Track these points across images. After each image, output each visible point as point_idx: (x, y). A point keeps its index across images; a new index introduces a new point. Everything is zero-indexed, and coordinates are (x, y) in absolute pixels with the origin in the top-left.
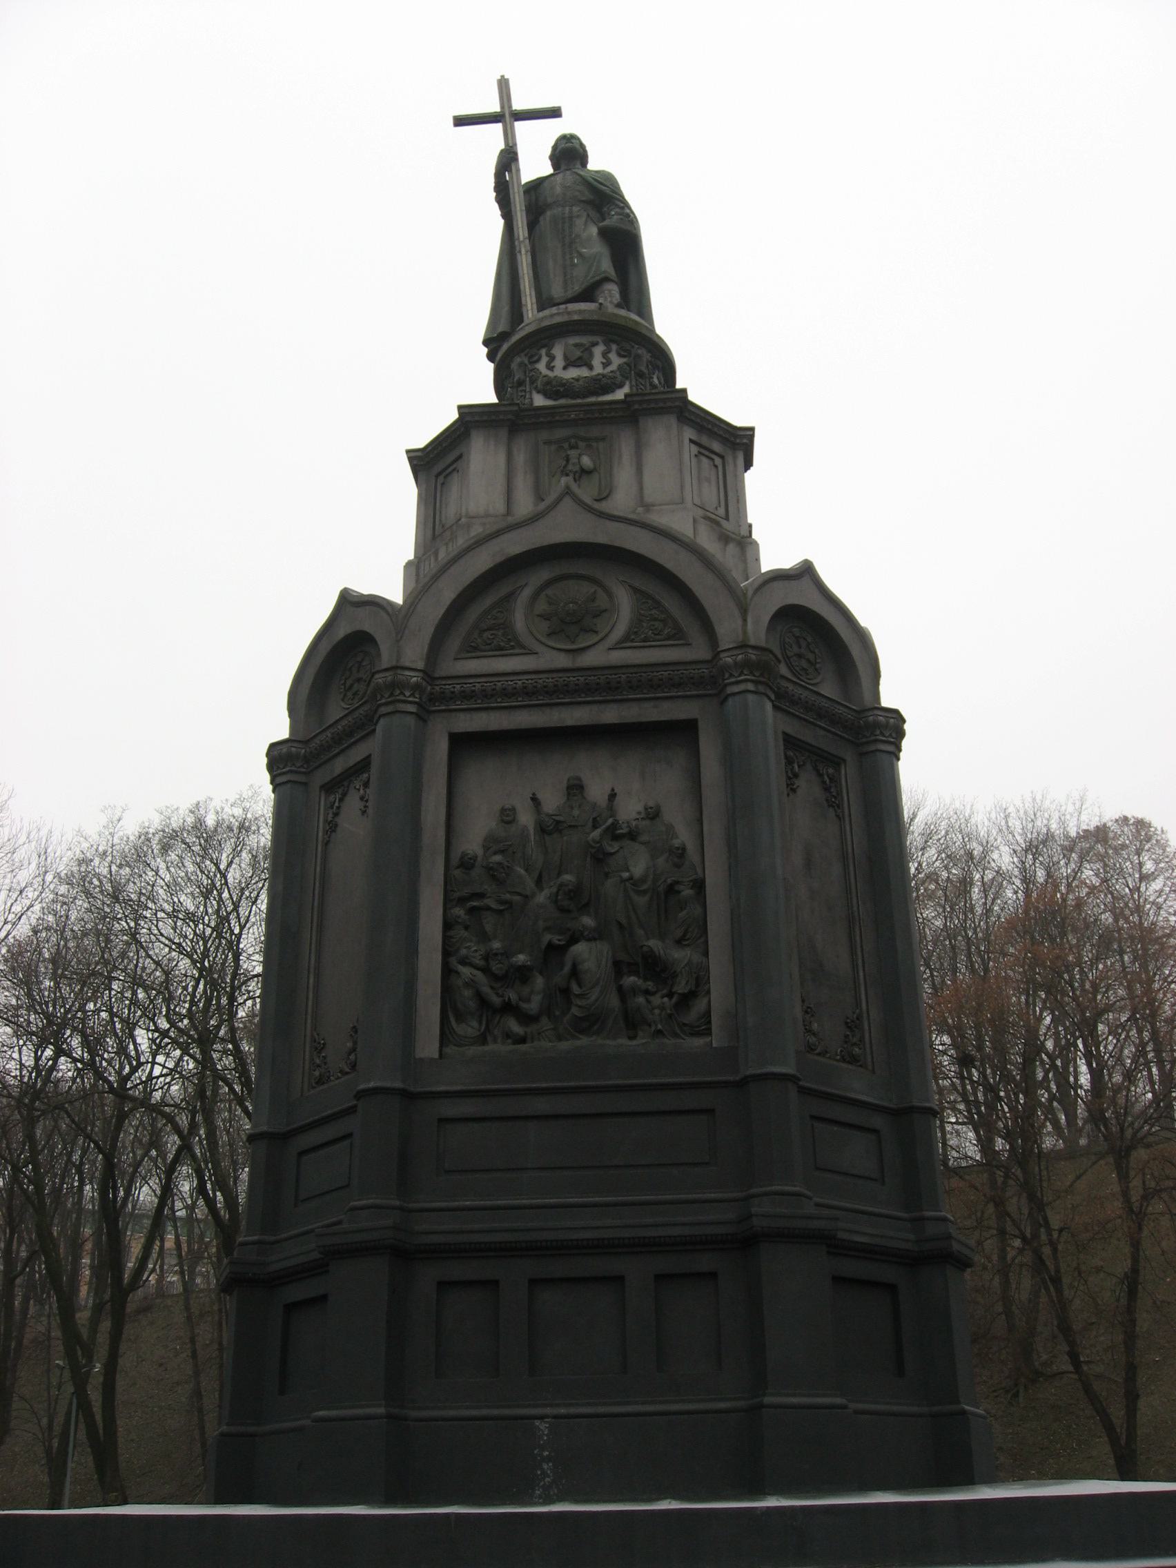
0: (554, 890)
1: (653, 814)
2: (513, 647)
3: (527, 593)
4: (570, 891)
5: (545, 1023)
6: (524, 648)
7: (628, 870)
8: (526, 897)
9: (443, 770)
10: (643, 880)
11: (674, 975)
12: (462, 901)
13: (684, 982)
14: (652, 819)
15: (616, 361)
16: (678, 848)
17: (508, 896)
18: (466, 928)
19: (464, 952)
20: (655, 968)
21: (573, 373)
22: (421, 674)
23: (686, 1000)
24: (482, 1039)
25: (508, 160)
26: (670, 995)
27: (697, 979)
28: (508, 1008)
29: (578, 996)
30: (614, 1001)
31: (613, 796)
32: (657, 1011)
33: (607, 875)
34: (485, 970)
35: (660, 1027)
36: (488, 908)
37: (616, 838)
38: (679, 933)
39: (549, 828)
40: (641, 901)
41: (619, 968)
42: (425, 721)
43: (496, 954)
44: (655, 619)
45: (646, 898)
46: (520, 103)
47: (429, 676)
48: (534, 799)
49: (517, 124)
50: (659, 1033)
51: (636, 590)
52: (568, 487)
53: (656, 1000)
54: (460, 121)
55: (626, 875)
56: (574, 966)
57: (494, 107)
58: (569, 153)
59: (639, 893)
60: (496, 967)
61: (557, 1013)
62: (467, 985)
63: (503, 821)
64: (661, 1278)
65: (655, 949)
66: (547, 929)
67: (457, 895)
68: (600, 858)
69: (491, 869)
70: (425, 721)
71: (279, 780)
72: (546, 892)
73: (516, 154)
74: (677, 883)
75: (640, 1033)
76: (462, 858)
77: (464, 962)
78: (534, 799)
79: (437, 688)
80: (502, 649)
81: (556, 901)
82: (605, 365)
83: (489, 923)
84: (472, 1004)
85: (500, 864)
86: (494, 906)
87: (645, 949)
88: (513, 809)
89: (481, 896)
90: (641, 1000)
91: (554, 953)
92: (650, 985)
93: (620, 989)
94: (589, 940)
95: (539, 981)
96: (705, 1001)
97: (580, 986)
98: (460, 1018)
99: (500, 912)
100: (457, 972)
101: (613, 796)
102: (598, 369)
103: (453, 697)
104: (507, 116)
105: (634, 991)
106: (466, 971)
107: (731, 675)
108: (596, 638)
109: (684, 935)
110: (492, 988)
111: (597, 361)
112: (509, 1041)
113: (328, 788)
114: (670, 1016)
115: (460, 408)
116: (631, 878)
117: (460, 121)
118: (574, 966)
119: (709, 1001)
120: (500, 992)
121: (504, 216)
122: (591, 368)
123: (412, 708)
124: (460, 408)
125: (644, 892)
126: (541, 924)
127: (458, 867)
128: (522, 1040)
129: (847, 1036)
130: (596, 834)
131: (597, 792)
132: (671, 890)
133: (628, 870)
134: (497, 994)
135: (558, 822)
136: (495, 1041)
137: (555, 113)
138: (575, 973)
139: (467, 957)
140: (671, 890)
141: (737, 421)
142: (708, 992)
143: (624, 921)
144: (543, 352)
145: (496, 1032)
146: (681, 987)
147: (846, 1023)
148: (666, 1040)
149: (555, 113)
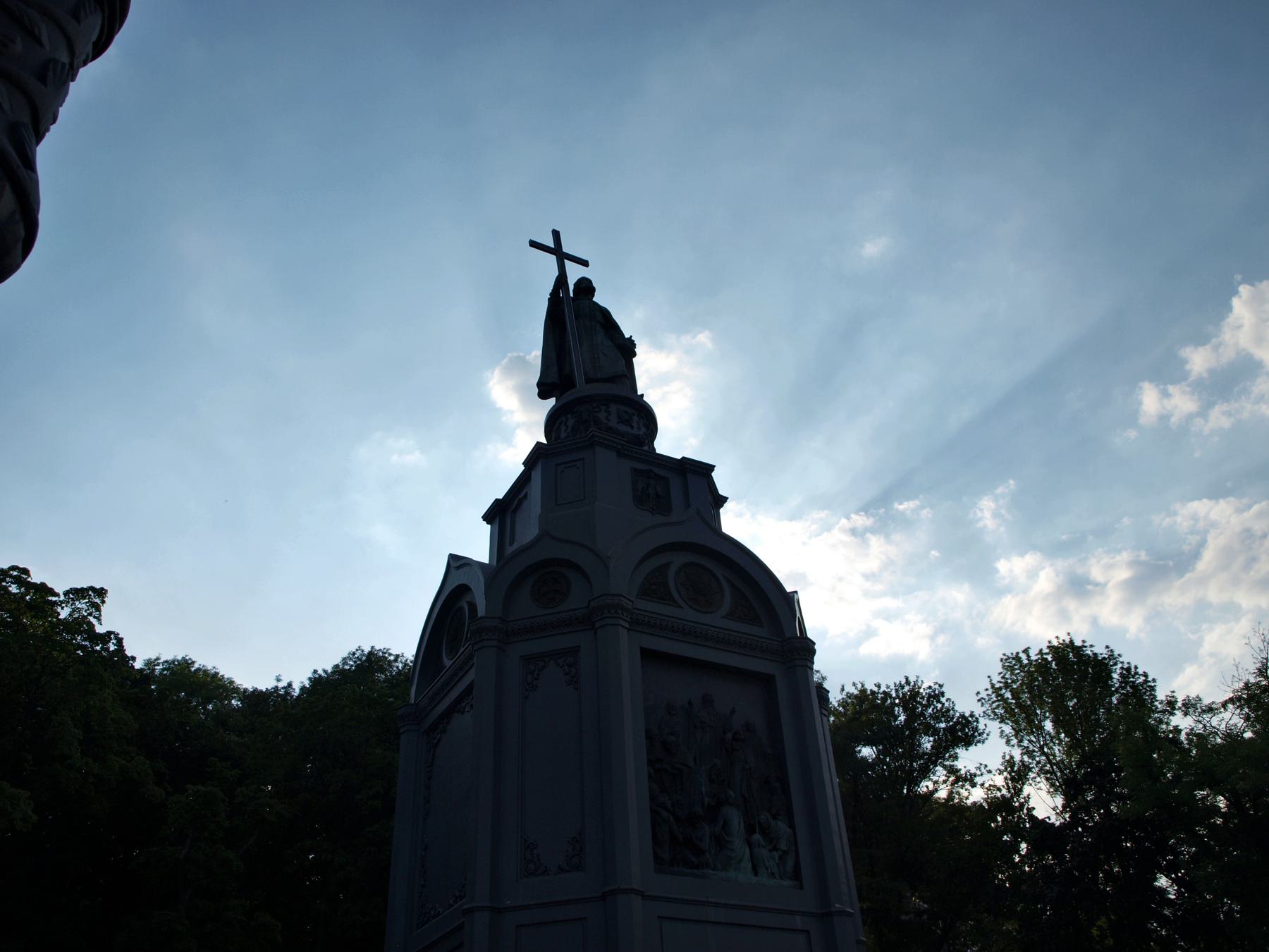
15: (643, 430)
21: (623, 428)
25: (561, 280)
46: (566, 249)
54: (534, 244)
57: (550, 243)
58: (585, 287)
82: (639, 429)
102: (635, 432)
111: (635, 425)
117: (534, 244)
122: (632, 427)
137: (585, 263)
141: (722, 491)
144: (604, 408)
149: (585, 263)
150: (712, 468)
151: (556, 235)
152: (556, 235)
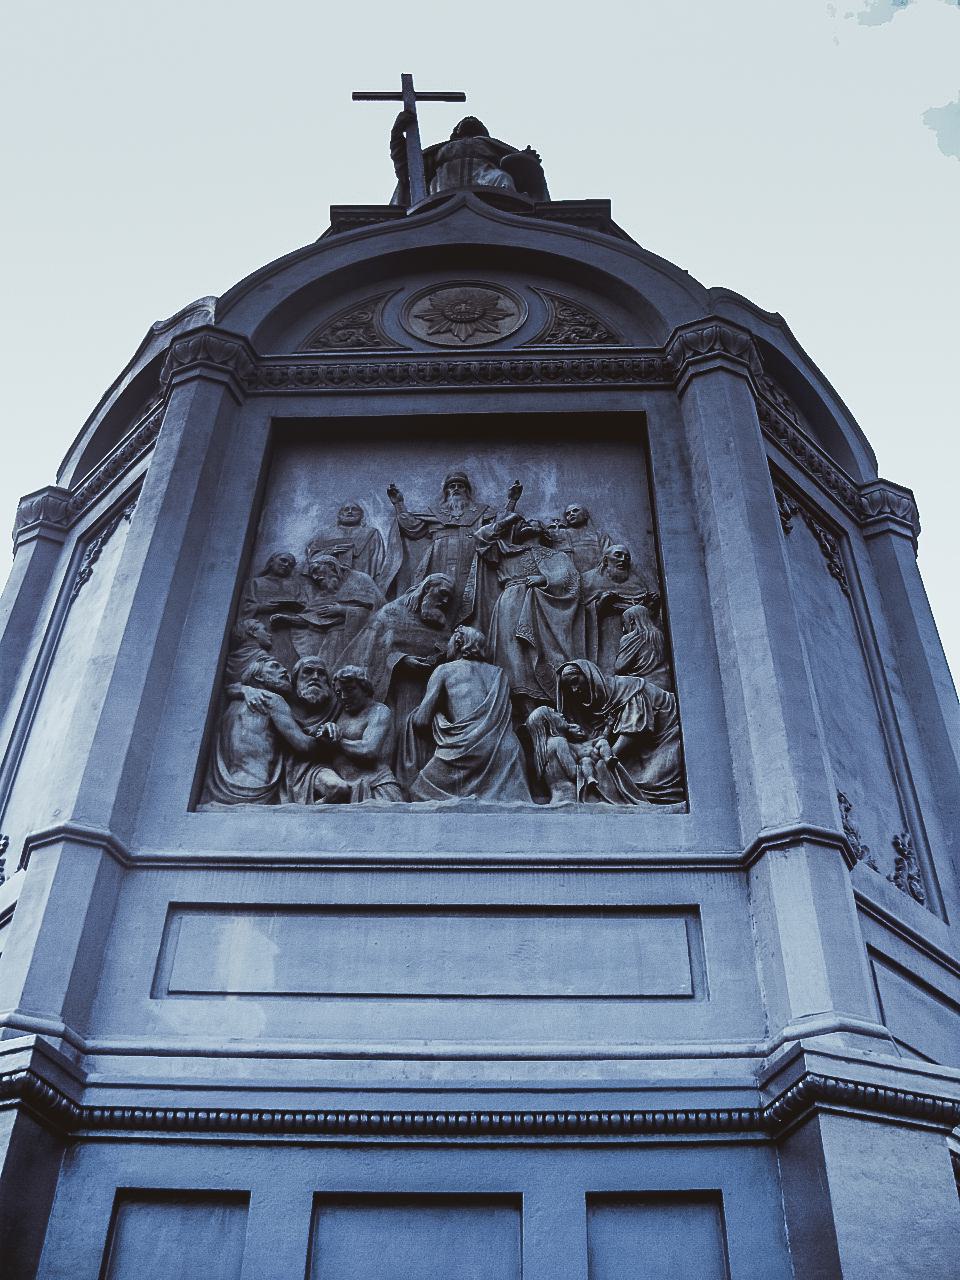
0: (416, 594)
1: (581, 522)
2: (378, 344)
3: (401, 297)
4: (443, 593)
5: (385, 776)
6: (393, 343)
7: (539, 573)
8: (369, 607)
9: (258, 458)
10: (565, 588)
11: (618, 708)
12: (261, 614)
13: (634, 717)
14: (577, 526)
16: (619, 554)
17: (339, 606)
18: (267, 648)
19: (255, 666)
20: (587, 707)
22: (241, 343)
23: (638, 748)
24: (271, 795)
26: (612, 739)
27: (658, 717)
28: (328, 752)
29: (447, 732)
30: (511, 743)
31: (516, 492)
32: (586, 760)
33: (502, 586)
34: (290, 695)
35: (591, 779)
36: (305, 625)
37: (521, 538)
38: (622, 661)
39: (413, 531)
40: (560, 616)
41: (520, 704)
42: (239, 404)
43: (309, 671)
44: (582, 324)
45: (570, 612)
47: (254, 354)
48: (393, 492)
49: (418, 104)
50: (591, 792)
51: (553, 298)
52: (464, 199)
53: (586, 748)
54: (357, 96)
55: (536, 579)
56: (443, 690)
59: (553, 602)
60: (305, 690)
61: (408, 765)
62: (254, 709)
63: (340, 523)
64: (597, 1201)
65: (586, 669)
66: (398, 645)
67: (253, 606)
68: (492, 563)
69: (315, 570)
70: (239, 404)
71: (21, 539)
72: (403, 598)
73: (414, 116)
74: (614, 599)
75: (556, 794)
76: (271, 560)
77: (254, 681)
78: (393, 492)
79: (264, 369)
80: (362, 344)
81: (419, 610)
83: (303, 642)
84: (262, 742)
85: (330, 564)
86: (315, 620)
87: (567, 670)
88: (361, 512)
89: (297, 608)
90: (556, 742)
91: (410, 678)
92: (575, 728)
93: (526, 737)
94: (471, 658)
95: (380, 712)
96: (674, 748)
97: (450, 719)
98: (234, 764)
99: (323, 630)
100: (241, 697)
101: (516, 492)
103: (284, 379)
104: (408, 94)
105: (547, 725)
106: (252, 694)
107: (696, 353)
108: (497, 337)
109: (635, 660)
110: (301, 725)
112: (321, 801)
113: (87, 538)
114: (612, 765)
115: (336, 211)
116: (544, 583)
117: (357, 96)
118: (443, 690)
119: (681, 752)
120: (311, 729)
121: (399, 172)
123: (225, 378)
124: (336, 211)
125: (567, 604)
126: (389, 637)
127: (263, 574)
128: (342, 796)
129: (897, 862)
130: (490, 528)
131: (491, 492)
132: (611, 607)
133: (539, 573)
134: (306, 732)
135: (428, 524)
136: (292, 800)
137: (459, 97)
138: (443, 704)
139: (259, 673)
140: (611, 607)
142: (679, 736)
143: (529, 637)
145: (296, 789)
146: (631, 721)
147: (895, 844)
148: (602, 803)
149: (459, 97)
150: (609, 201)
151: (407, 79)
152: (407, 79)
